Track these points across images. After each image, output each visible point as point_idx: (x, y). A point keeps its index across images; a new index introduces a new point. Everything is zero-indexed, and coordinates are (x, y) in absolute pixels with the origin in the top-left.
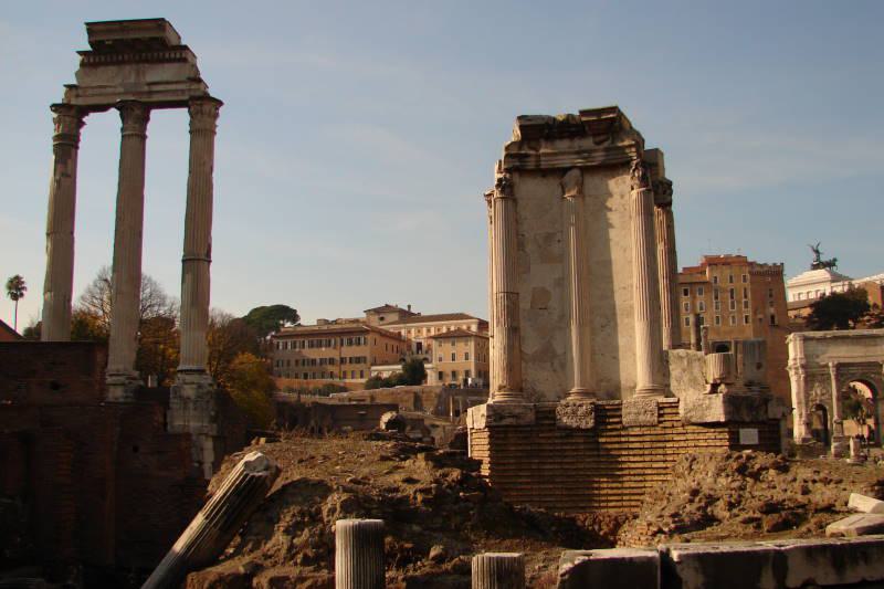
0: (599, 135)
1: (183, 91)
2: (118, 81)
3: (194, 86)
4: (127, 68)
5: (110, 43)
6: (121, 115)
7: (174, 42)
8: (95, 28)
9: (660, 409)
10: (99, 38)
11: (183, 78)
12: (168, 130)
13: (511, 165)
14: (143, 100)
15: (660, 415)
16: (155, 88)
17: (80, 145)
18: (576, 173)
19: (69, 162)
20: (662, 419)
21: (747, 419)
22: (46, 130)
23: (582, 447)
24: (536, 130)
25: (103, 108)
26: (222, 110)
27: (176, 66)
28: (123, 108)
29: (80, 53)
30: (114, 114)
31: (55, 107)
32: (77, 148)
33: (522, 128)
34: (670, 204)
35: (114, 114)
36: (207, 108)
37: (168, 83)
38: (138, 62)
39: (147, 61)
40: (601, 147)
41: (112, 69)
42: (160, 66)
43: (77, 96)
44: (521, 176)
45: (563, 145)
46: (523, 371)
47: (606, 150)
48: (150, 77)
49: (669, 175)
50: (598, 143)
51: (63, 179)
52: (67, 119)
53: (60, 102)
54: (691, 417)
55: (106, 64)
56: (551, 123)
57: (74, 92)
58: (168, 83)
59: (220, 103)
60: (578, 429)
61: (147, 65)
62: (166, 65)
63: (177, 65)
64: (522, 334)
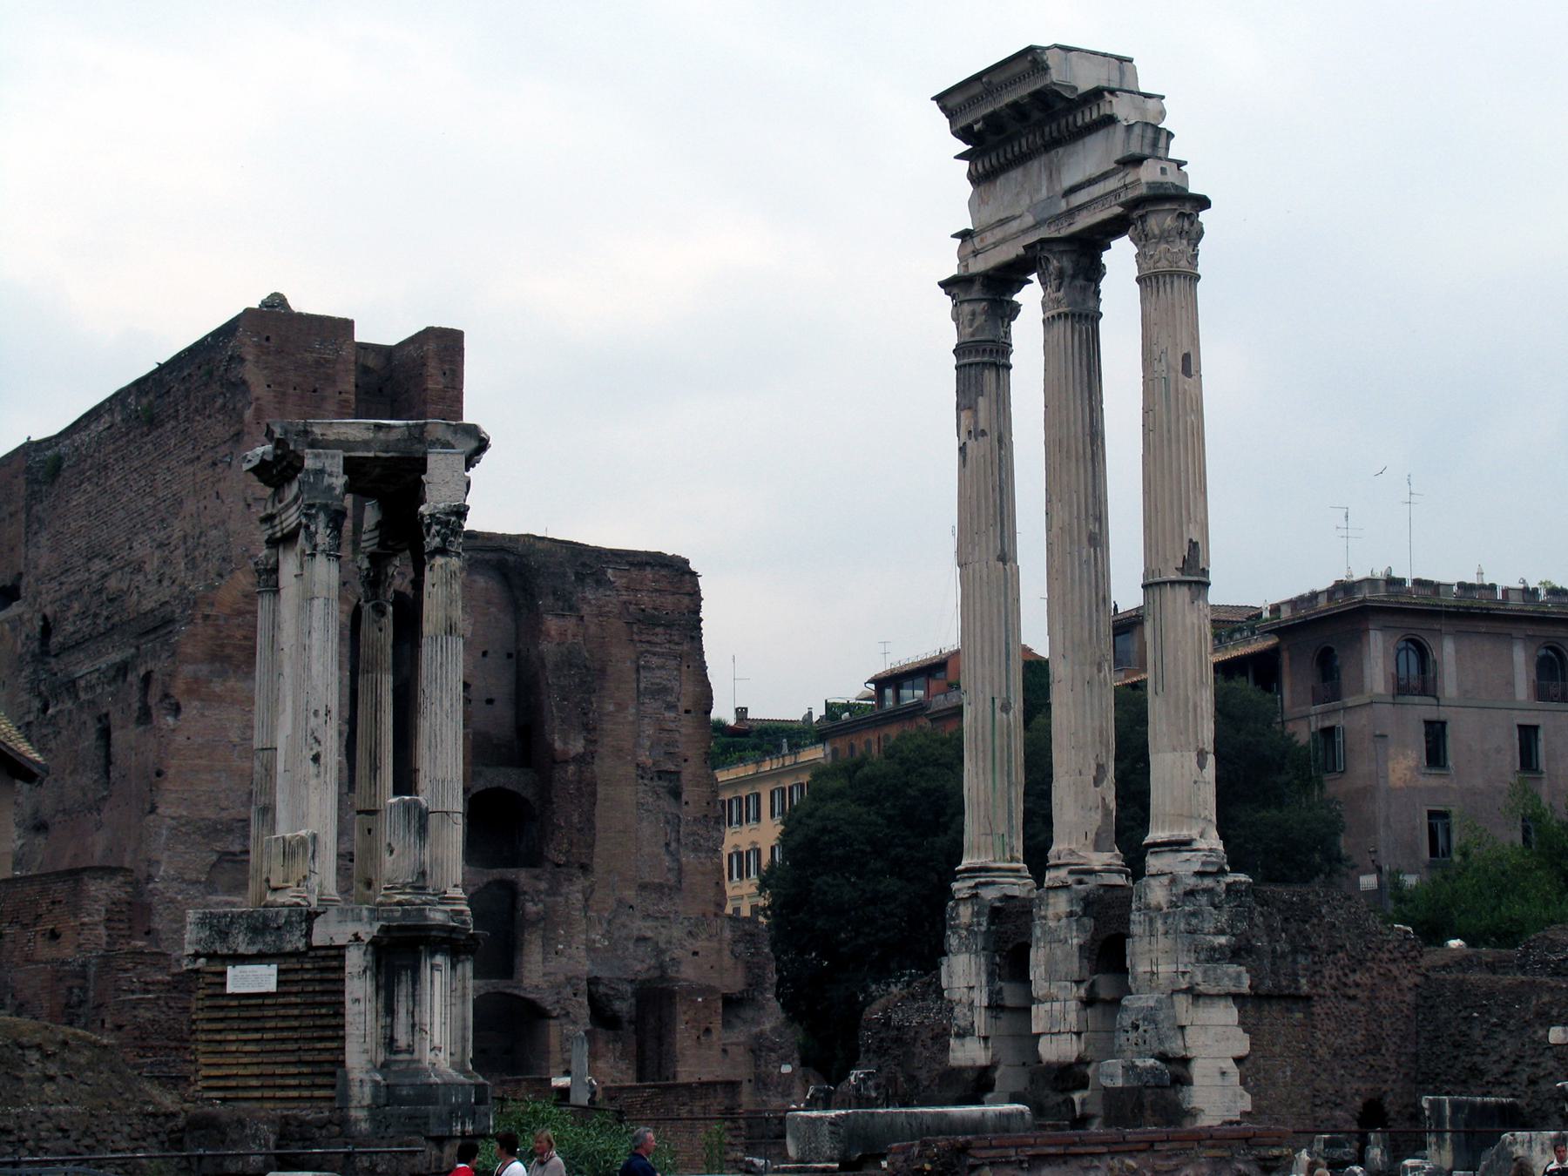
2: (1025, 201)
4: (1035, 165)
8: (951, 103)
14: (1064, 232)
17: (1013, 359)
21: (242, 950)
29: (960, 157)
37: (1091, 182)
43: (976, 253)
48: (1070, 178)
51: (971, 444)
53: (951, 269)
58: (1091, 182)
61: (1061, 150)
63: (1102, 134)
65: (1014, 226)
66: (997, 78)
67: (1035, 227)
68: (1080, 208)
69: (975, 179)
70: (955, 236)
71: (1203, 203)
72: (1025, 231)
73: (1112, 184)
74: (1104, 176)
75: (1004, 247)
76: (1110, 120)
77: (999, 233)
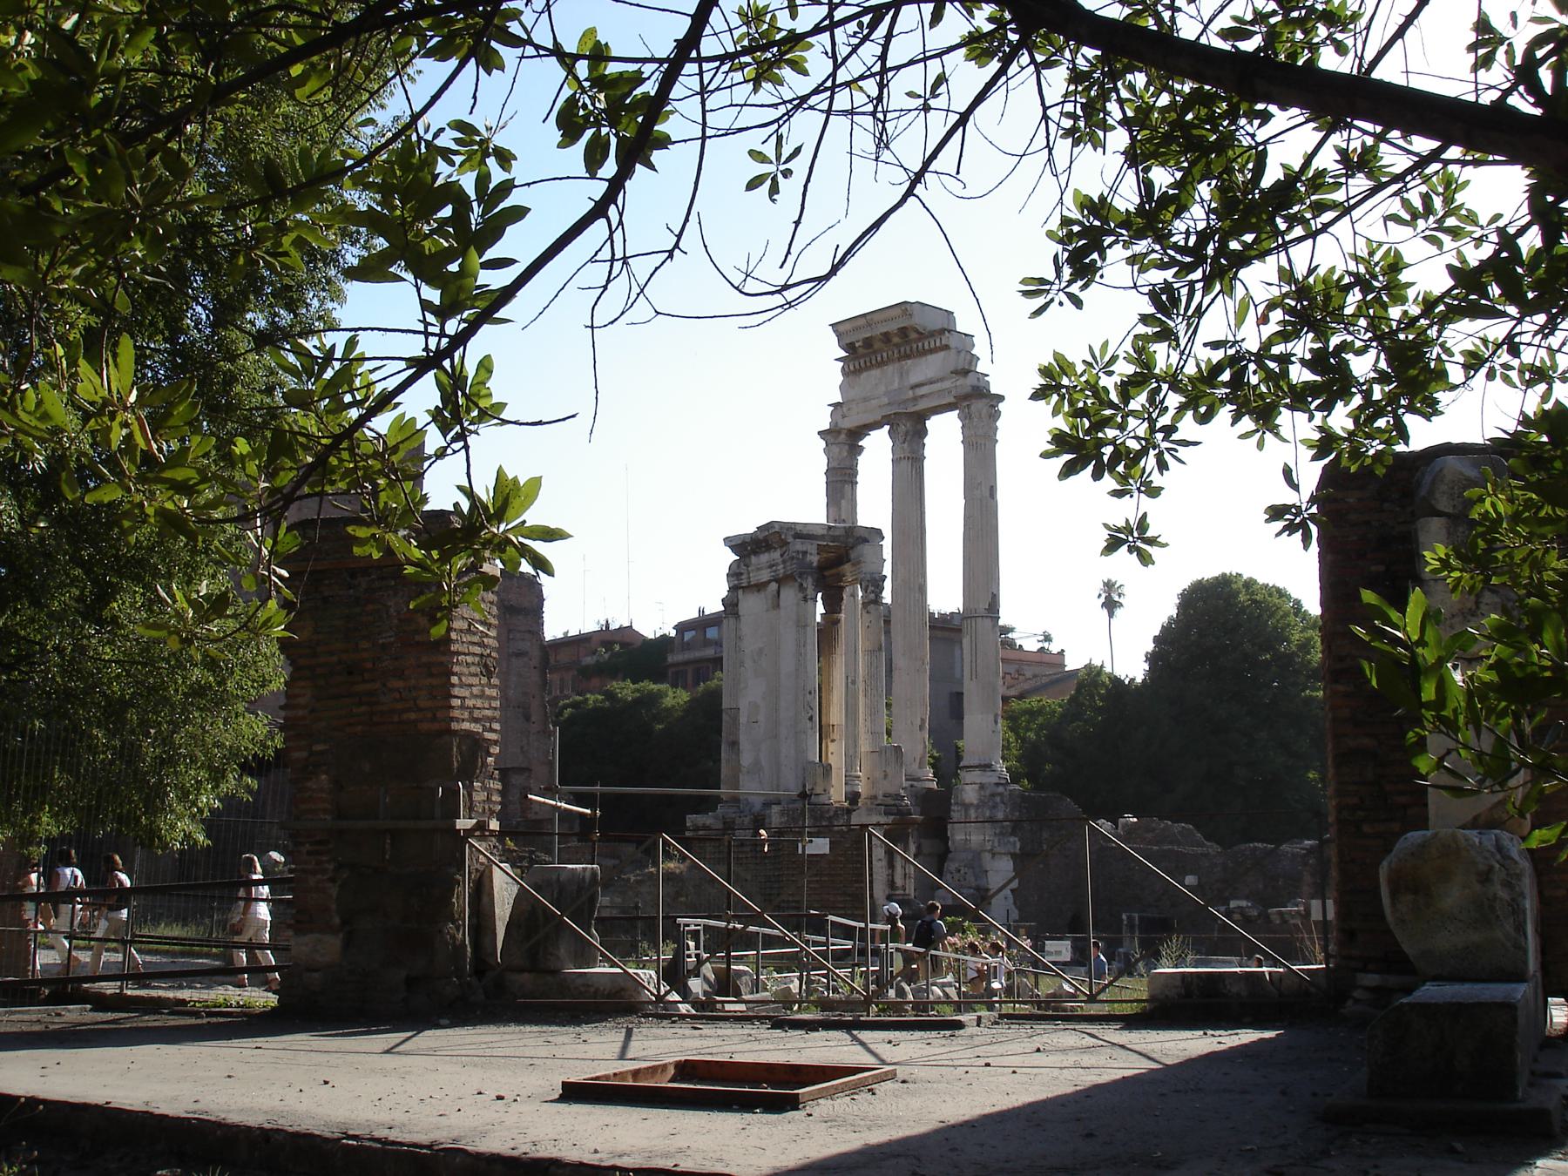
2: (882, 389)
3: (961, 381)
4: (890, 369)
8: (841, 328)
18: (774, 586)
22: (816, 461)
25: (876, 425)
26: (1001, 406)
28: (892, 421)
36: (978, 406)
38: (900, 359)
39: (908, 357)
41: (875, 373)
48: (914, 380)
52: (836, 449)
55: (867, 368)
57: (839, 411)
59: (1001, 398)
62: (930, 358)
63: (942, 354)
66: (876, 317)
71: (1001, 398)
73: (947, 384)
74: (941, 380)
76: (947, 347)
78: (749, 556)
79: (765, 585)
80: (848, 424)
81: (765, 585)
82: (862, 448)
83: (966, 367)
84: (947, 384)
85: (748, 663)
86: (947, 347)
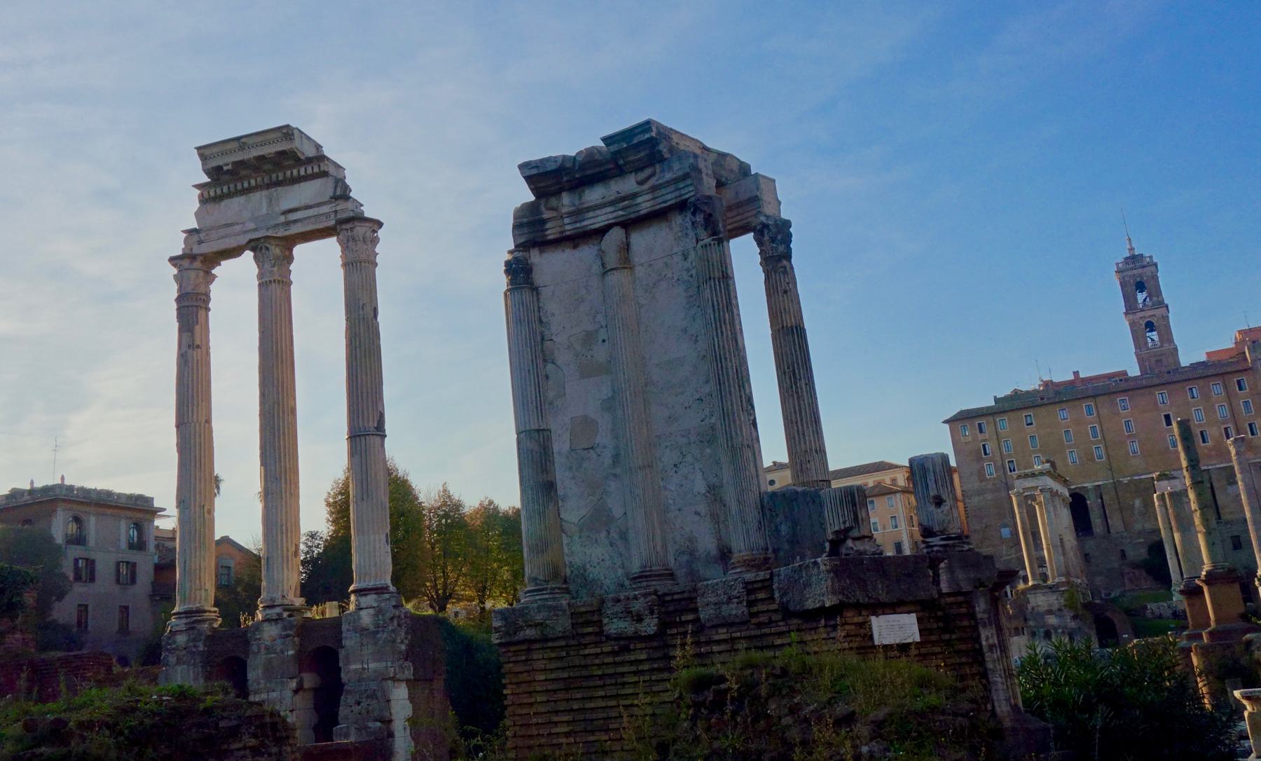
0: (641, 169)
1: (327, 215)
3: (342, 205)
4: (257, 196)
5: (230, 167)
6: (255, 257)
7: (310, 152)
8: (207, 152)
9: (749, 592)
10: (214, 163)
11: (327, 198)
12: (317, 266)
13: (522, 240)
15: (750, 604)
16: (292, 217)
17: (211, 305)
18: (616, 234)
19: (197, 328)
20: (755, 609)
21: (883, 597)
23: (646, 667)
24: (549, 179)
25: (233, 252)
27: (317, 183)
28: (255, 246)
29: (198, 186)
30: (248, 255)
31: (173, 260)
32: (208, 309)
33: (530, 179)
34: (788, 256)
35: (248, 255)
36: (360, 230)
39: (278, 184)
40: (646, 186)
42: (296, 187)
43: (200, 242)
44: (541, 252)
45: (594, 195)
46: (566, 550)
47: (654, 189)
49: (784, 215)
50: (640, 183)
54: (788, 602)
55: (230, 195)
56: (569, 165)
57: (195, 238)
59: (380, 224)
60: (637, 637)
64: (561, 492)
65: (237, 228)
66: (250, 141)
67: (255, 230)
68: (295, 221)
69: (204, 200)
70: (184, 232)
72: (245, 232)
73: (325, 209)
75: (227, 240)
76: (325, 174)
77: (222, 232)
78: (557, 193)
79: (602, 232)
80: (205, 249)
81: (602, 232)
82: (214, 277)
83: (342, 193)
84: (325, 209)
85: (563, 357)
86: (325, 174)
